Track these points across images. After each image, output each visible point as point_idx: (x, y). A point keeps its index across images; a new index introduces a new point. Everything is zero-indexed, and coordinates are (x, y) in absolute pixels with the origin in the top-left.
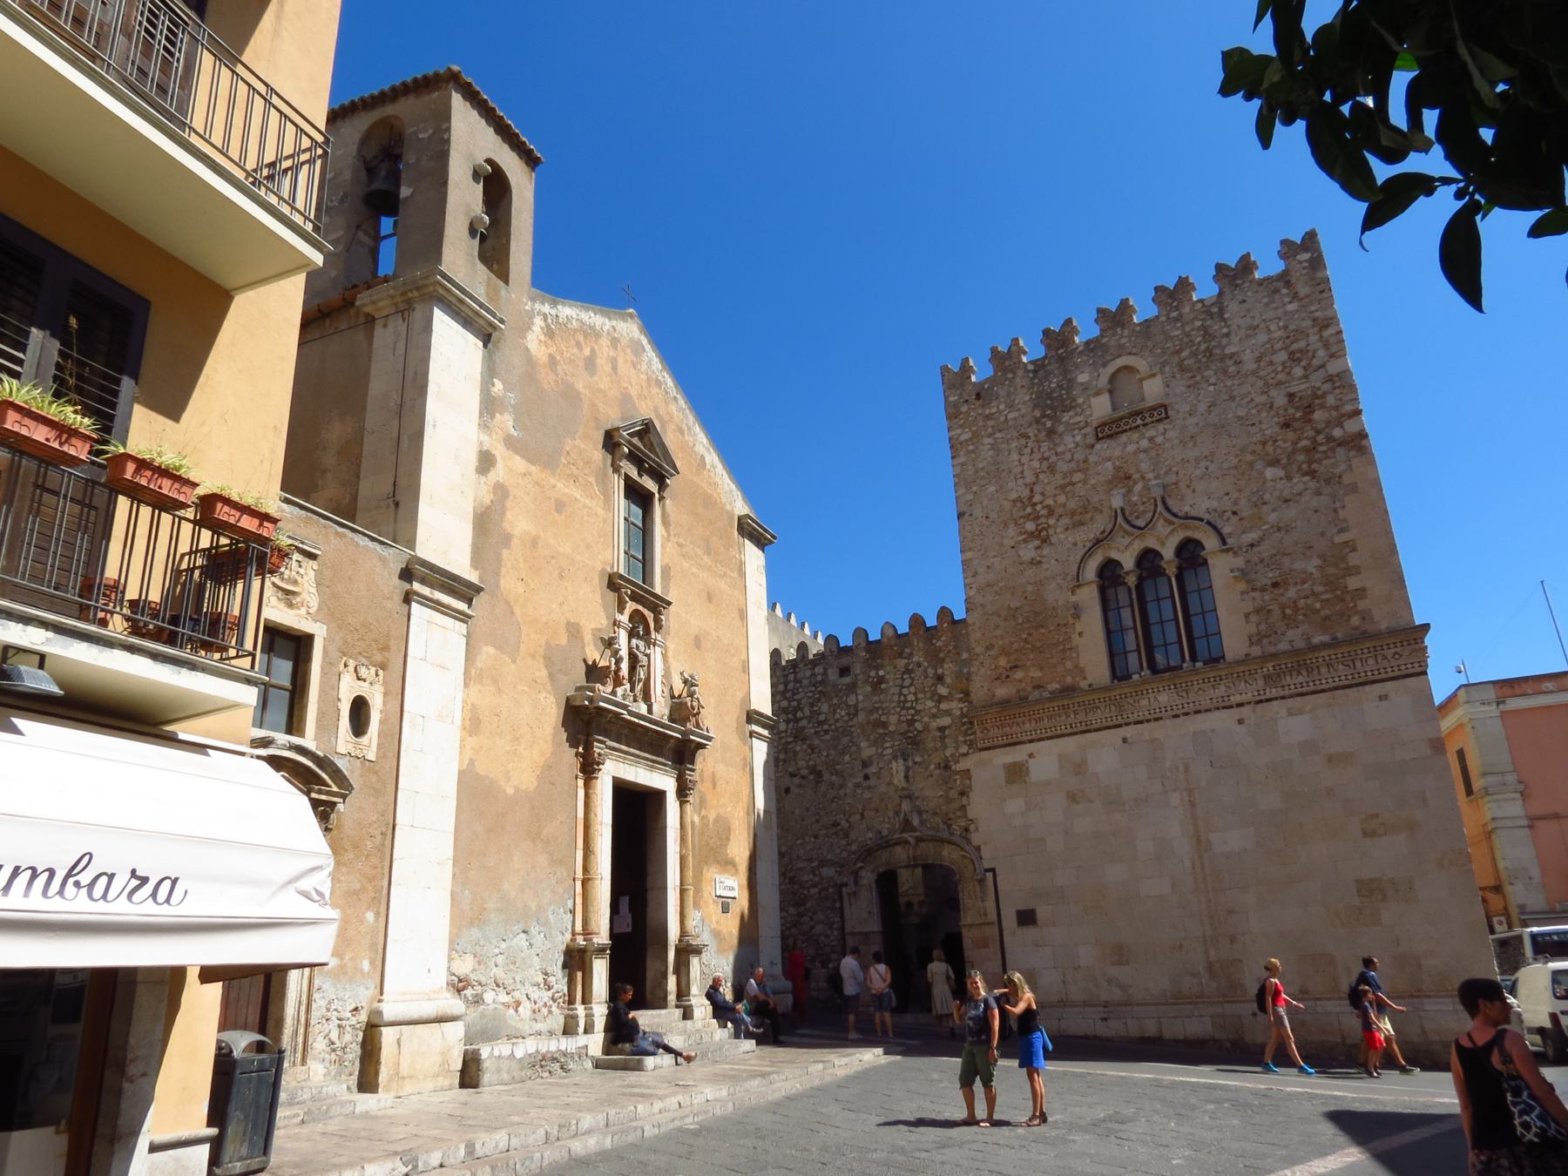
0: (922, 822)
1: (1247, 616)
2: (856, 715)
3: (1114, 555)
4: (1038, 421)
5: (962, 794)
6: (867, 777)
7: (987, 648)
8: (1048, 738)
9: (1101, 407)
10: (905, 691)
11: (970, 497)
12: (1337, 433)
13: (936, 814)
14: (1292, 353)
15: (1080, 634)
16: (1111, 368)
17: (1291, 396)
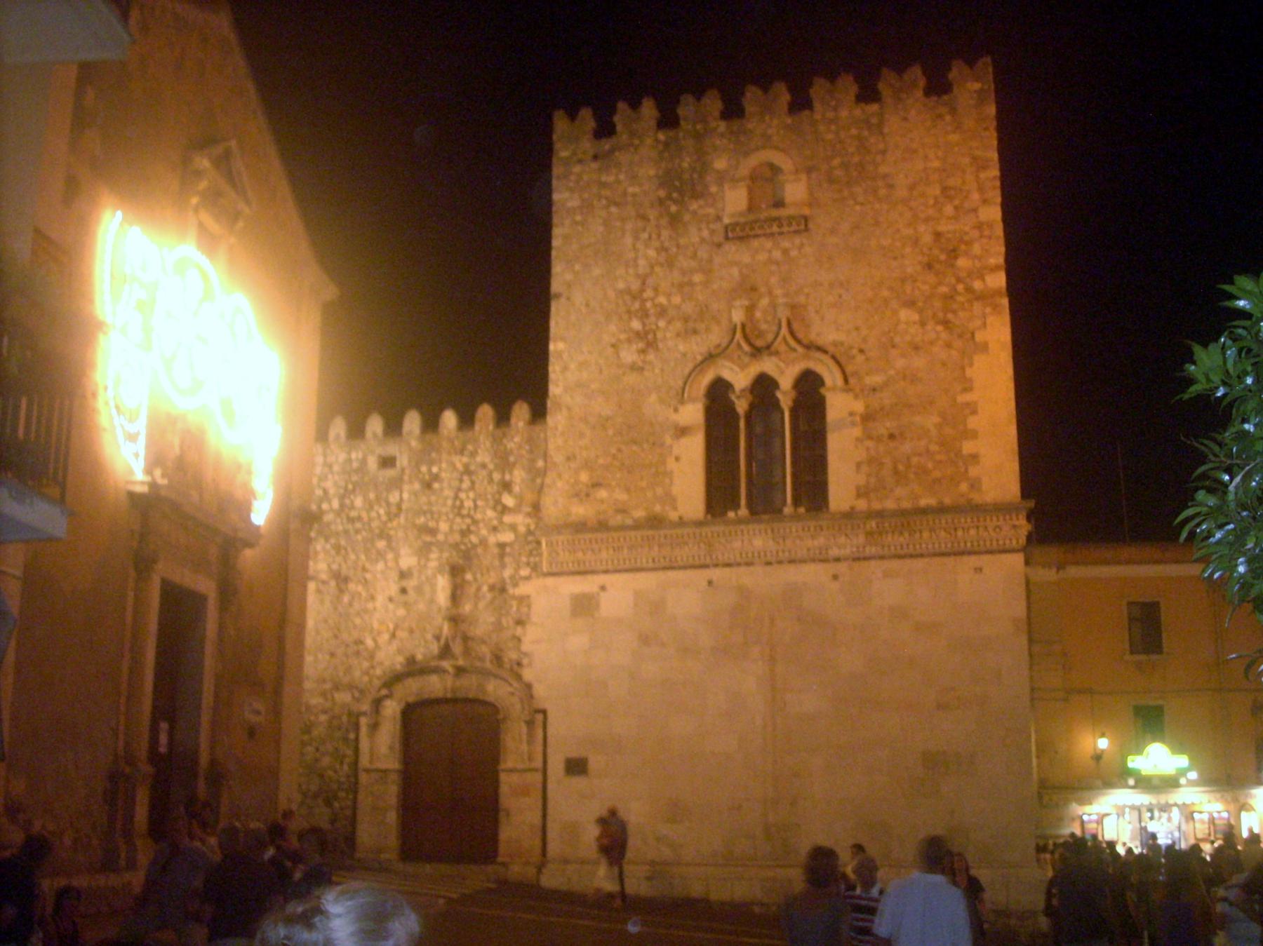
1: (859, 465)
3: (727, 375)
4: (661, 202)
5: (519, 623)
7: (568, 459)
8: (627, 571)
10: (463, 495)
12: (977, 285)
13: (484, 642)
14: (945, 189)
15: (677, 459)
17: (938, 235)
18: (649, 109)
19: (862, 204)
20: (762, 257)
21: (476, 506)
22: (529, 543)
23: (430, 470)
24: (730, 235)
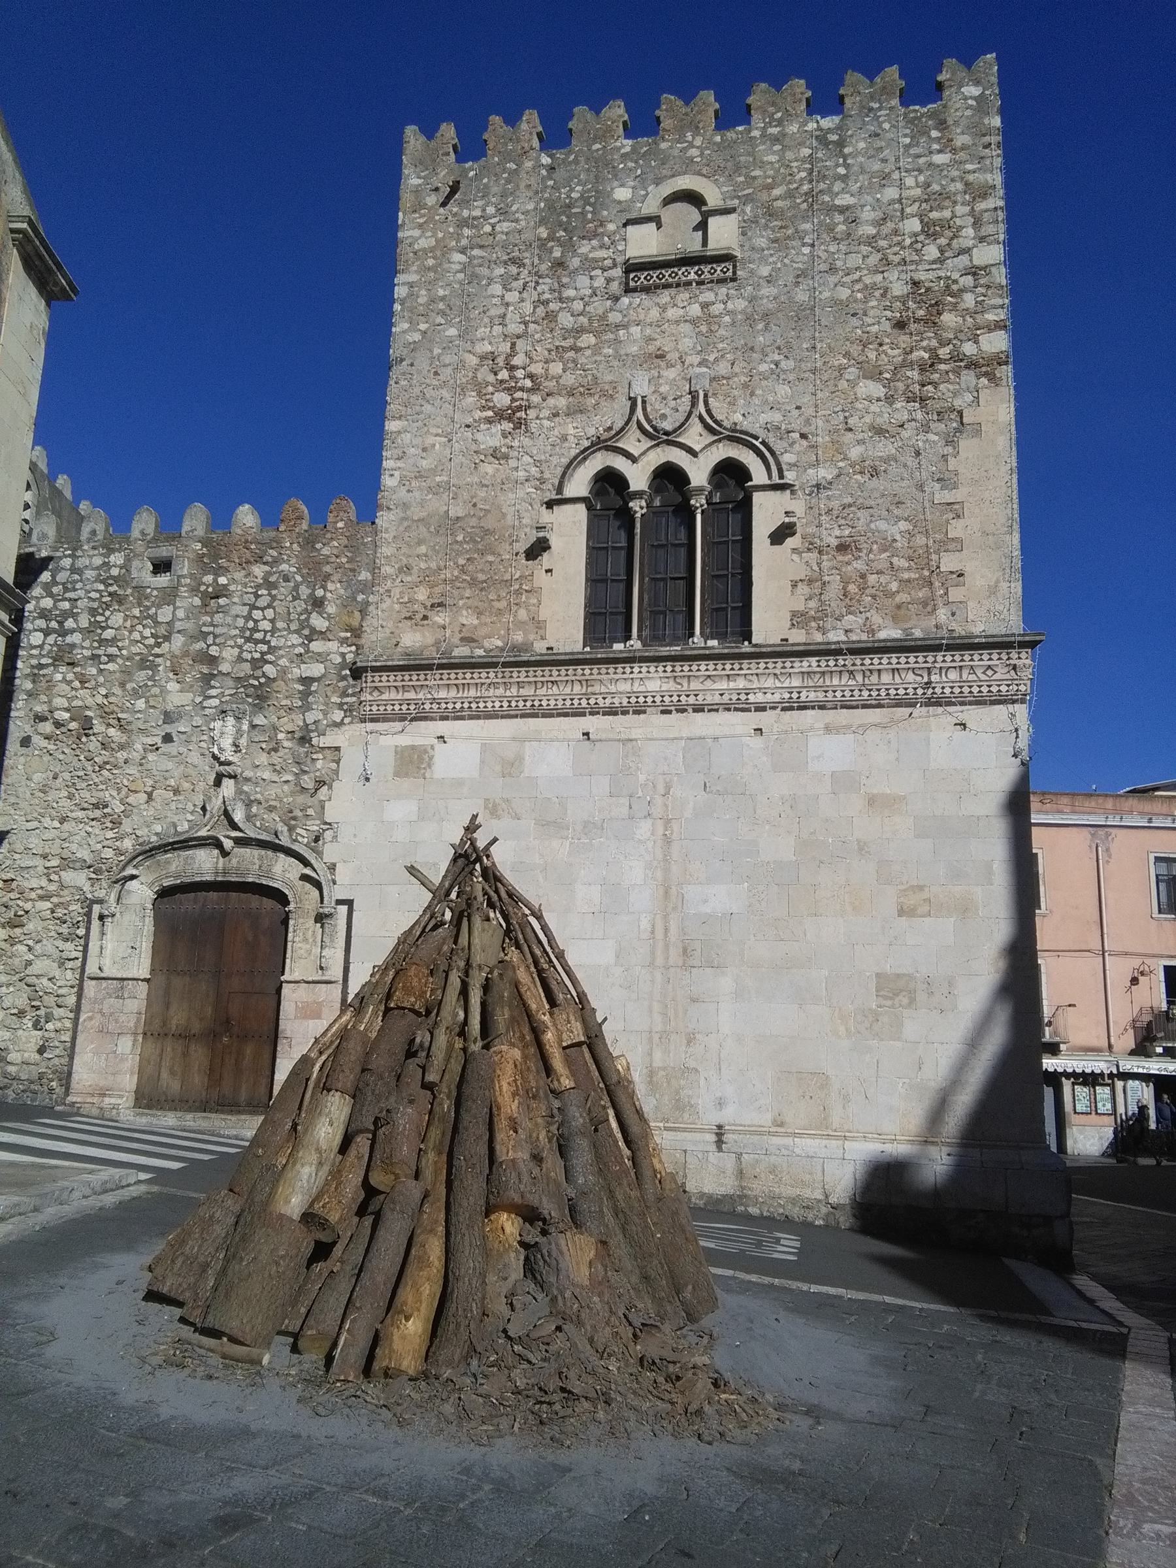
0: (249, 818)
2: (167, 638)
3: (620, 463)
4: (542, 244)
6: (168, 738)
7: (400, 570)
9: (644, 243)
11: (417, 337)
12: (969, 349)
16: (667, 189)
18: (530, 123)
19: (813, 245)
20: (672, 313)
21: (274, 630)
22: (344, 678)
23: (215, 580)
24: (632, 284)
